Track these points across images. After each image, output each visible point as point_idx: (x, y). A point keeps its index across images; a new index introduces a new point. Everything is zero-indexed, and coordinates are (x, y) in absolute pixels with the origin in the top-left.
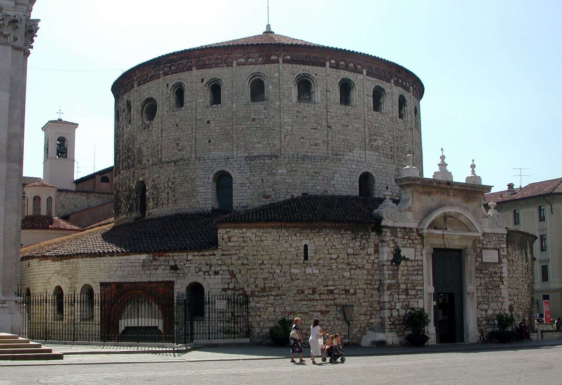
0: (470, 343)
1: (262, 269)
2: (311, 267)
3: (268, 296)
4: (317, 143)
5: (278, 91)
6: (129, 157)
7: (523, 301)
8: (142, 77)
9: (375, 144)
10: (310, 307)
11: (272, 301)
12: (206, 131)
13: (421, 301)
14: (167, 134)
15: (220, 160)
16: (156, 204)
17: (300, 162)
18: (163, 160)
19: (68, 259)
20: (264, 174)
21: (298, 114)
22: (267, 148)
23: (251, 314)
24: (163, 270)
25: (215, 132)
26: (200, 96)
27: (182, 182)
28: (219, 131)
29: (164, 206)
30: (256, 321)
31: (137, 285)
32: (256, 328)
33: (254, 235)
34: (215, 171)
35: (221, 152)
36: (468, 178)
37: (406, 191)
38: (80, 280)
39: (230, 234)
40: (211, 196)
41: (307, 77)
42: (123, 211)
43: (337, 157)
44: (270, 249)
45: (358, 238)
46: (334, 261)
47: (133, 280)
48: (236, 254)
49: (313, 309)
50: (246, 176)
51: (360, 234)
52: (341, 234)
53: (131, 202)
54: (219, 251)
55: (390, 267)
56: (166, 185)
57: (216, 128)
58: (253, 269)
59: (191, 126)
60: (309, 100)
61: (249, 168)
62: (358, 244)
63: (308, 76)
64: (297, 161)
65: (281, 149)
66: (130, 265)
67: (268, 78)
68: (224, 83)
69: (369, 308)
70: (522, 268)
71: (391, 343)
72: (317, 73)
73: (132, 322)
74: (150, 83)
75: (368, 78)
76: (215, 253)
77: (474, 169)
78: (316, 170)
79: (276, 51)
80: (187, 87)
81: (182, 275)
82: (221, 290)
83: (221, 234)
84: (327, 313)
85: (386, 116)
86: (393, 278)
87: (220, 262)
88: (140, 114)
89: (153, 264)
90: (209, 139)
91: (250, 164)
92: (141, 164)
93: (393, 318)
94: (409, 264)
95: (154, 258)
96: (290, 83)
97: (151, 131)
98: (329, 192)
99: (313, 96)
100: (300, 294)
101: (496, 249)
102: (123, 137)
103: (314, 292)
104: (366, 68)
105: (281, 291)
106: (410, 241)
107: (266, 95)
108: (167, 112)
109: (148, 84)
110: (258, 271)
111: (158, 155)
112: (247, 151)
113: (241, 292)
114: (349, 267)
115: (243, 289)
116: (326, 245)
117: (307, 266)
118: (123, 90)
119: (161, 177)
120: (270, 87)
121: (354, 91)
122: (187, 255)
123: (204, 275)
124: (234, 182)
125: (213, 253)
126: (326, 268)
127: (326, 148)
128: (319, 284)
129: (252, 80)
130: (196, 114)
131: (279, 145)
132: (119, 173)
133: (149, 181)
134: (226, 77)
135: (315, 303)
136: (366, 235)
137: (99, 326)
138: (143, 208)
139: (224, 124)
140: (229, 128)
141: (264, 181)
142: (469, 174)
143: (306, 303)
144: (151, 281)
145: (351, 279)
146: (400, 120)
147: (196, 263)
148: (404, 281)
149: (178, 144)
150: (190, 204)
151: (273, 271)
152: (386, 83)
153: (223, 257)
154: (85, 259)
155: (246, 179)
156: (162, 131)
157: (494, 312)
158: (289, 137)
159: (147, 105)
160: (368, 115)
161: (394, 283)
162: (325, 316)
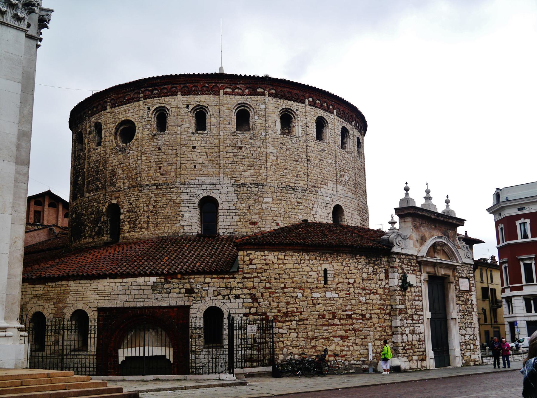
0: (457, 367)
1: (285, 293)
3: (291, 321)
5: (264, 122)
6: (98, 180)
8: (117, 100)
9: (343, 179)
10: (331, 333)
11: (295, 327)
12: (191, 156)
13: (422, 325)
14: (147, 157)
15: (206, 186)
16: (133, 227)
20: (251, 202)
22: (254, 177)
26: (185, 121)
27: (165, 206)
28: (205, 157)
29: (143, 230)
32: (280, 356)
33: (276, 257)
34: (201, 196)
37: (406, 220)
38: (70, 305)
39: (251, 256)
42: (87, 235)
45: (371, 263)
46: (351, 286)
47: (139, 304)
48: (258, 277)
51: (373, 259)
52: (357, 259)
54: (239, 273)
55: (400, 292)
56: (145, 208)
57: (202, 153)
60: (289, 133)
62: (371, 269)
65: (267, 178)
66: (136, 287)
69: (383, 333)
71: (404, 369)
72: (297, 108)
73: (136, 352)
74: (128, 105)
75: (338, 118)
77: (449, 204)
79: (262, 84)
81: (199, 299)
86: (402, 304)
87: (240, 285)
88: (113, 136)
91: (237, 191)
93: (404, 342)
94: (412, 289)
96: (274, 115)
101: (467, 278)
103: (334, 318)
104: (336, 109)
106: (412, 268)
107: (251, 124)
108: (148, 135)
111: (137, 178)
114: (364, 292)
115: (265, 314)
116: (343, 270)
118: (90, 112)
121: (327, 129)
122: (205, 278)
123: (224, 299)
124: (220, 208)
125: (233, 276)
126: (344, 292)
127: (306, 180)
129: (238, 110)
132: (83, 196)
135: (336, 329)
136: (378, 260)
137: (95, 357)
141: (251, 208)
143: (327, 328)
144: (162, 305)
145: (366, 303)
147: (214, 286)
148: (409, 307)
149: (160, 168)
151: (295, 295)
152: (350, 125)
153: (244, 280)
154: (77, 282)
155: (232, 205)
158: (274, 167)
159: (122, 127)
161: (403, 308)
162: (344, 341)
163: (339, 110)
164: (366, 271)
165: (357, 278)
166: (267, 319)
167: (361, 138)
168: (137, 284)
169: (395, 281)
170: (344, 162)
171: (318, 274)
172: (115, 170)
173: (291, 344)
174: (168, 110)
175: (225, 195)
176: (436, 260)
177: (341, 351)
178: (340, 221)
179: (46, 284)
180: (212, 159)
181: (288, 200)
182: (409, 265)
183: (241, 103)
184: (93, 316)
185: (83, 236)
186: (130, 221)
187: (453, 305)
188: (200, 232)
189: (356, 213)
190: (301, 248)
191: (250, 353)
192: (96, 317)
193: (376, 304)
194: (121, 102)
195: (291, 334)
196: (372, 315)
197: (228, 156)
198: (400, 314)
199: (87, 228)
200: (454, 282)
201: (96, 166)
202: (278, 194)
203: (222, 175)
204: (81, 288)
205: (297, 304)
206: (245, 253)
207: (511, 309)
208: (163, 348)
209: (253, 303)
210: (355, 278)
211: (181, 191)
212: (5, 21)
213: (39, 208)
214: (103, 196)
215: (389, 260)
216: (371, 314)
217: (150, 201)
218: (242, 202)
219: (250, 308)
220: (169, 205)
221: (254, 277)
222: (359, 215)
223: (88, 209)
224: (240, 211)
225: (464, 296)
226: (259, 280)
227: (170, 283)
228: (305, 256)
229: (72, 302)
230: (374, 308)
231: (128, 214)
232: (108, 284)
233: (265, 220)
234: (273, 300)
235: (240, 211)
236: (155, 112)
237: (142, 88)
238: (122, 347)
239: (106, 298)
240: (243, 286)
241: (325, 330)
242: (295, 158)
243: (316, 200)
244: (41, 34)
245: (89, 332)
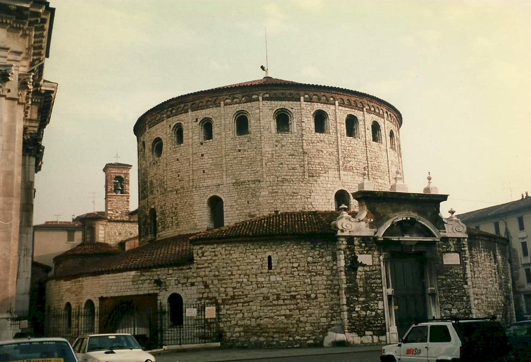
1: (231, 279)
2: (275, 275)
3: (237, 303)
7: (494, 299)
10: (275, 312)
11: (241, 308)
13: (380, 303)
23: (223, 320)
25: (207, 163)
26: (196, 133)
27: (182, 207)
28: (211, 162)
29: (169, 229)
30: (227, 325)
32: (227, 333)
33: (224, 249)
34: (209, 197)
40: (206, 218)
44: (237, 261)
46: (295, 269)
47: (125, 294)
48: (208, 267)
49: (278, 313)
51: (319, 244)
52: (301, 245)
54: (194, 264)
56: (170, 210)
57: (209, 159)
70: (490, 269)
72: (292, 107)
75: (340, 108)
76: (191, 267)
78: (295, 191)
79: (256, 91)
80: (184, 125)
82: (196, 300)
83: (196, 250)
84: (292, 317)
87: (195, 275)
96: (269, 117)
97: (159, 166)
98: (307, 209)
100: (265, 300)
103: (278, 299)
105: (248, 298)
107: (250, 129)
109: (155, 126)
113: (214, 300)
114: (310, 274)
117: (271, 275)
119: (167, 204)
120: (252, 122)
122: (168, 270)
123: (182, 286)
124: (224, 205)
128: (283, 291)
129: (238, 117)
138: (155, 232)
141: (250, 202)
142: (426, 185)
145: (311, 284)
147: (175, 277)
149: (179, 176)
151: (241, 280)
152: (359, 112)
156: (166, 165)
157: (458, 311)
159: (156, 144)
160: (341, 140)
164: (310, 255)
165: (301, 262)
170: (350, 148)
171: (262, 261)
176: (399, 238)
183: (240, 111)
184: (97, 304)
193: (322, 284)
196: (318, 295)
197: (229, 159)
203: (224, 177)
206: (199, 248)
209: (205, 289)
210: (299, 263)
216: (316, 294)
218: (243, 198)
219: (203, 293)
220: (185, 207)
226: (209, 269)
227: (144, 275)
230: (319, 288)
237: (165, 109)
238: (121, 326)
239: (104, 290)
241: (270, 310)
243: (313, 189)
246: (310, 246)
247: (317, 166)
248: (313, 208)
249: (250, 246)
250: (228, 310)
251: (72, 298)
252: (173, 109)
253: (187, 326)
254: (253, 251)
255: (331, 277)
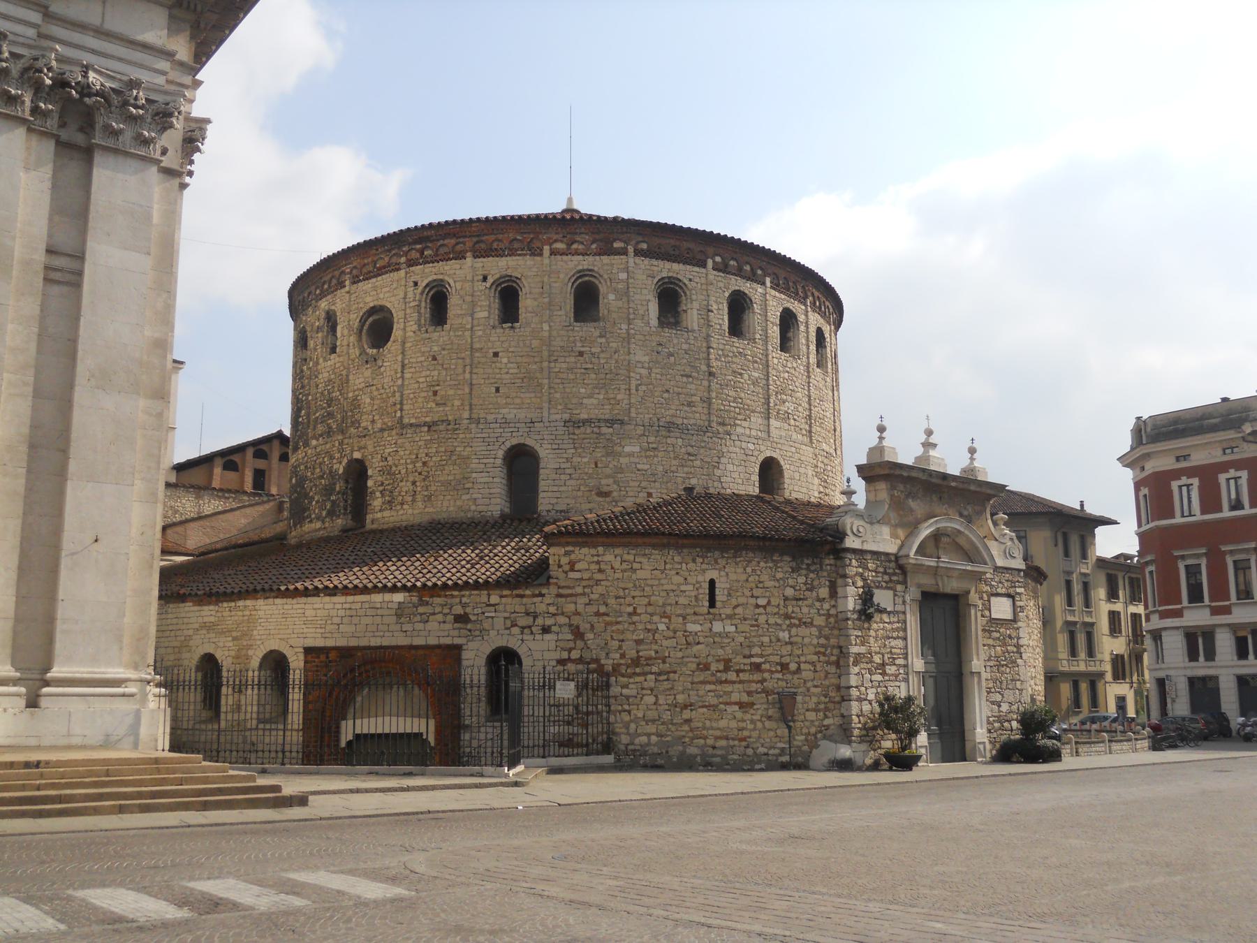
1: (634, 623)
2: (722, 620)
3: (644, 674)
4: (692, 402)
5: (626, 305)
6: (331, 415)
11: (652, 684)
12: (490, 371)
15: (517, 425)
16: (389, 502)
17: (664, 433)
18: (406, 421)
19: (234, 601)
21: (660, 349)
22: (605, 407)
24: (440, 623)
25: (507, 373)
26: (481, 306)
28: (515, 371)
29: (405, 507)
30: (622, 720)
31: (385, 653)
32: (623, 737)
33: (619, 558)
34: (508, 445)
35: (519, 410)
36: (964, 471)
37: (877, 488)
38: (259, 642)
39: (573, 557)
40: (498, 490)
41: (675, 283)
42: (313, 516)
43: (725, 428)
44: (648, 585)
45: (802, 569)
46: (761, 610)
47: (375, 642)
48: (584, 594)
50: (565, 456)
51: (806, 561)
52: (773, 561)
53: (333, 498)
57: (512, 365)
58: (618, 623)
59: (460, 361)
61: (571, 441)
62: (802, 580)
63: (677, 282)
64: (658, 431)
65: (629, 409)
67: (608, 280)
68: (526, 285)
69: (823, 699)
72: (691, 277)
74: (379, 278)
75: (773, 292)
76: (544, 591)
78: (690, 450)
79: (623, 233)
81: (477, 633)
82: (554, 663)
84: (751, 708)
85: (799, 362)
87: (552, 609)
89: (419, 611)
90: (496, 385)
91: (574, 434)
92: (357, 428)
93: (864, 716)
95: (420, 599)
96: (645, 291)
97: (380, 367)
99: (684, 318)
101: (1008, 595)
102: (316, 377)
103: (727, 669)
104: (769, 275)
105: (668, 665)
106: (886, 578)
107: (603, 310)
108: (414, 332)
109: (374, 280)
110: (626, 626)
111: (395, 412)
112: (568, 411)
113: (593, 666)
114: (788, 622)
115: (597, 661)
116: (747, 580)
118: (318, 292)
120: (612, 297)
122: (489, 595)
123: (522, 633)
124: (542, 465)
125: (540, 592)
126: (746, 622)
127: (706, 411)
129: (578, 282)
130: (471, 338)
131: (625, 402)
132: (306, 444)
133: (374, 460)
134: (529, 274)
136: (815, 564)
137: (301, 734)
139: (525, 360)
140: (534, 367)
141: (599, 465)
142: (965, 462)
143: (712, 687)
144: (414, 644)
145: (791, 643)
146: (818, 370)
147: (505, 611)
149: (435, 393)
150: (459, 503)
151: (654, 627)
153: (560, 600)
154: (271, 601)
156: (403, 366)
158: (644, 388)
159: (371, 319)
161: (864, 651)
162: (746, 712)
163: (775, 278)
164: (790, 584)
165: (773, 595)
166: (600, 670)
167: (827, 329)
168: (372, 605)
169: (851, 600)
172: (359, 398)
173: (644, 716)
174: (450, 285)
175: (552, 441)
177: (739, 730)
178: (776, 486)
179: (220, 604)
180: (528, 375)
181: (670, 449)
182: (879, 572)
183: (583, 270)
184: (296, 662)
185: (307, 517)
186: (384, 490)
187: (978, 649)
188: (507, 510)
189: (810, 472)
190: (665, 541)
191: (571, 731)
192: (302, 664)
193: (810, 644)
194: (370, 272)
195: (645, 697)
197: (557, 370)
198: (856, 663)
199: (314, 503)
200: (980, 603)
201: (328, 390)
202: (652, 439)
204: (277, 612)
205: (656, 643)
206: (562, 551)
207: (1159, 656)
208: (416, 720)
210: (769, 597)
211: (472, 436)
212: (121, 147)
213: (261, 464)
214: (339, 445)
215: (839, 563)
216: (799, 663)
217: (417, 455)
218: (584, 454)
219: (570, 650)
220: (450, 462)
221: (576, 595)
222: (817, 475)
223: (314, 468)
224: (579, 471)
225: (1001, 630)
226: (585, 600)
227: (427, 603)
228: (673, 556)
229: (263, 637)
231: (380, 478)
232: (321, 606)
233: (625, 487)
234: (612, 636)
235: (579, 471)
236: (427, 290)
237: (404, 245)
240: (557, 609)
242: (684, 371)
244: (192, 162)
245: (291, 690)
246: (791, 563)
247: (731, 404)
248: (723, 488)
249: (674, 556)
250: (625, 686)
251: (221, 644)
252: (427, 248)
253: (531, 719)
254: (680, 567)
255: (826, 631)
